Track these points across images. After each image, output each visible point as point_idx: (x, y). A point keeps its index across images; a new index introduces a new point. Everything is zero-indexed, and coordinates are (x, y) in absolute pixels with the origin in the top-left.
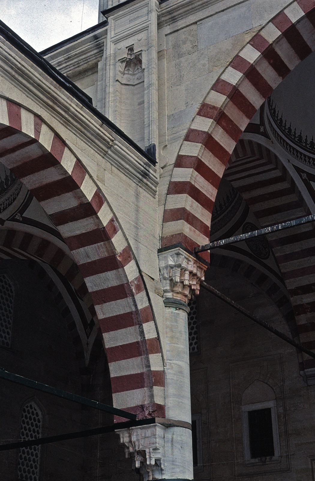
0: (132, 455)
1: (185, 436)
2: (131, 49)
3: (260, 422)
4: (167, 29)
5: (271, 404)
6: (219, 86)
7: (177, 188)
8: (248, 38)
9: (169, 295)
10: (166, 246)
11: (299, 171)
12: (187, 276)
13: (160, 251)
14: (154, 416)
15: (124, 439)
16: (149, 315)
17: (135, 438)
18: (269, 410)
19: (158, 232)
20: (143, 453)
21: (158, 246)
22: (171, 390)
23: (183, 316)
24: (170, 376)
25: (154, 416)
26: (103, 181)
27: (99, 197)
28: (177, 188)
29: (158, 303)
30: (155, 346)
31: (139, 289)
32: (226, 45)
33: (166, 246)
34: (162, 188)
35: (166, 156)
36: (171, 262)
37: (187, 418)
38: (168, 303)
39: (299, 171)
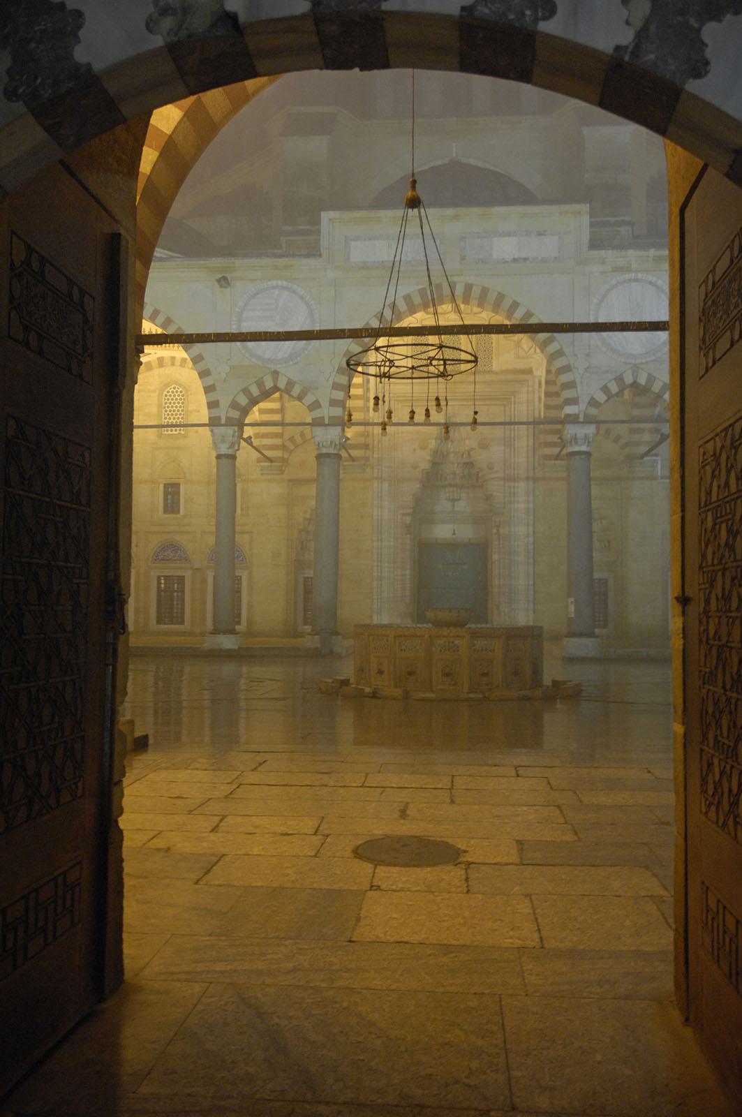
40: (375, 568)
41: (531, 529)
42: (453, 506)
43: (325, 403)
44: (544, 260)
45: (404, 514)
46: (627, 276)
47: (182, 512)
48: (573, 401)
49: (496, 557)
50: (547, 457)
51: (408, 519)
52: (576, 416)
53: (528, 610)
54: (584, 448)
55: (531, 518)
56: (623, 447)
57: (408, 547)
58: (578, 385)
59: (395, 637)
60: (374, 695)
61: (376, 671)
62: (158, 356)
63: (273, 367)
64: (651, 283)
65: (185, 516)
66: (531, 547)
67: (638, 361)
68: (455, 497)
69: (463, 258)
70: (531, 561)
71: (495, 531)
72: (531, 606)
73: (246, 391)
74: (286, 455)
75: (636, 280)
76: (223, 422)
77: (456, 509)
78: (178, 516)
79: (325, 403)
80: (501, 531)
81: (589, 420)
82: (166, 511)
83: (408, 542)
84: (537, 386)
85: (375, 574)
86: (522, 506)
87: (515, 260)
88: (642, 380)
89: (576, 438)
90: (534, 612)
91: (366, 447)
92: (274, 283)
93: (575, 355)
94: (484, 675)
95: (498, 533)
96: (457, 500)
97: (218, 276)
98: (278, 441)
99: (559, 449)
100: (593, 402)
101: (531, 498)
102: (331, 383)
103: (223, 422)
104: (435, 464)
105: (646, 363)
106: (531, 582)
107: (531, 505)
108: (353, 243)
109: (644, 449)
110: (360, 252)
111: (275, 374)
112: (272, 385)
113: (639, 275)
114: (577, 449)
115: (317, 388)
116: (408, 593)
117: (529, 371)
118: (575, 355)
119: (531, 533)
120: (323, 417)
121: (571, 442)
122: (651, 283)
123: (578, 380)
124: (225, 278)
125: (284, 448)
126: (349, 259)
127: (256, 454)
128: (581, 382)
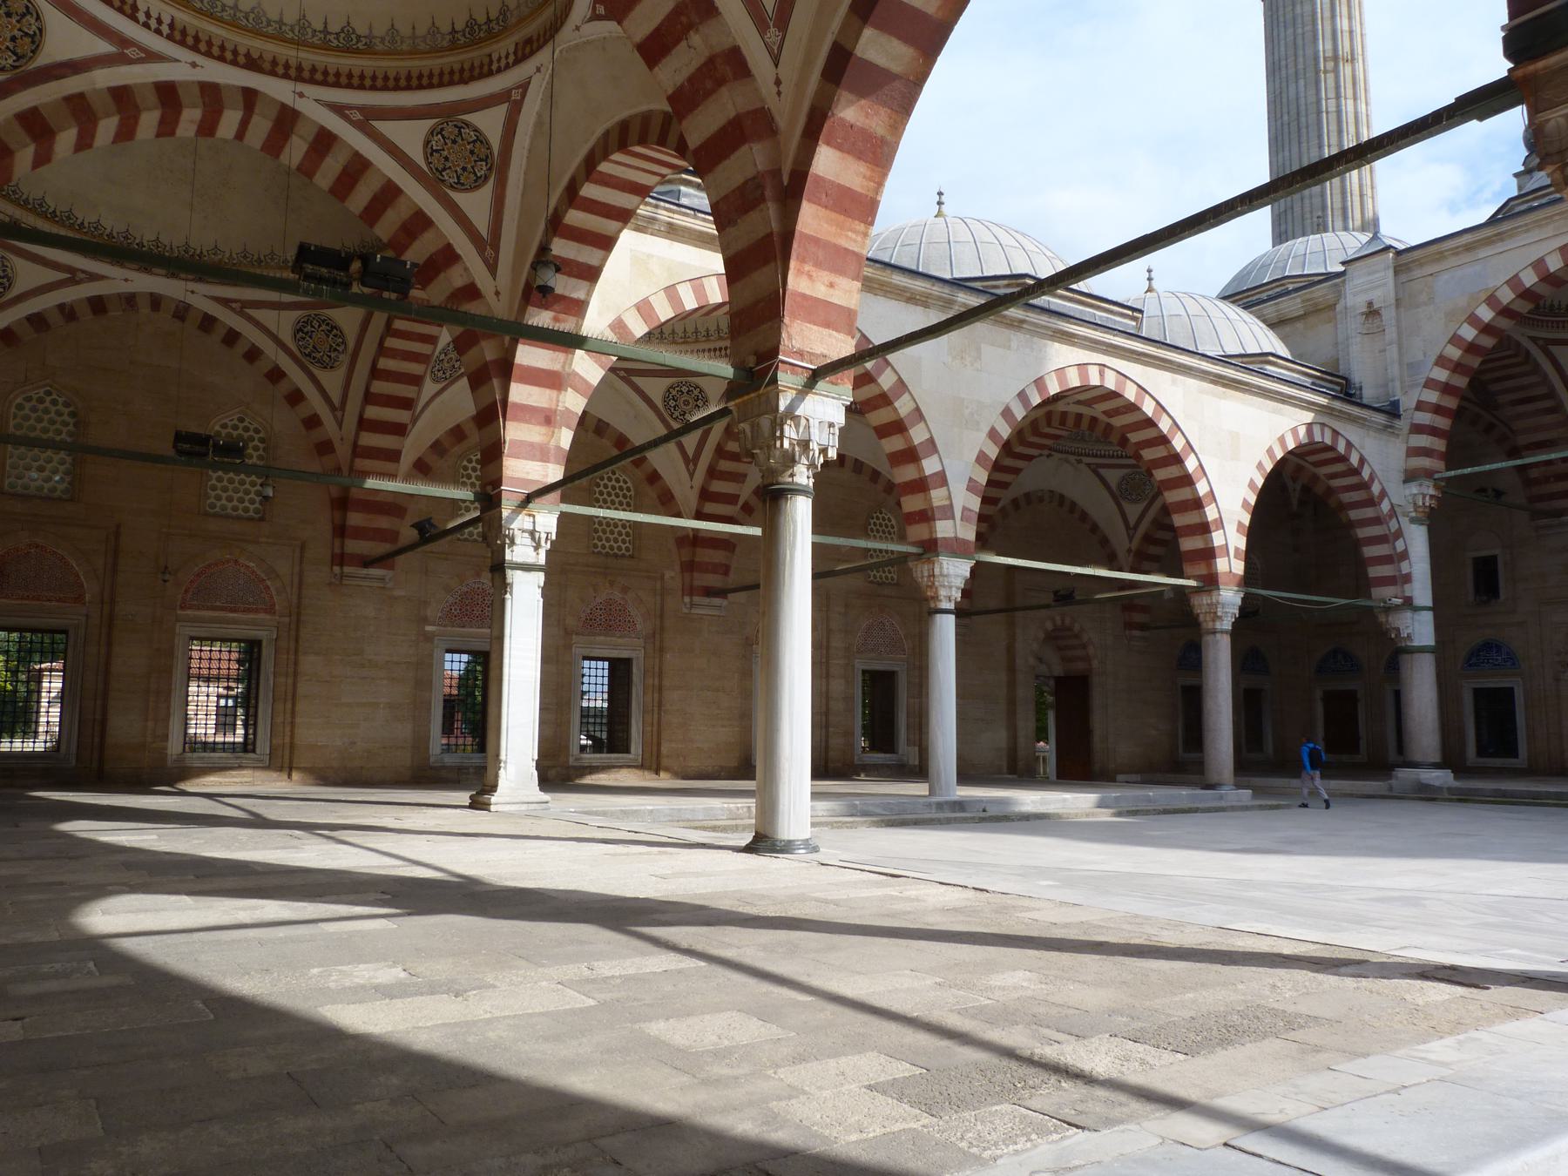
1: (1427, 618)
7: (1417, 429)
10: (1410, 477)
11: (1534, 339)
15: (1382, 618)
16: (1399, 534)
18: (1495, 557)
27: (1362, 461)
28: (1417, 429)
29: (1404, 521)
30: (1404, 556)
31: (1391, 517)
33: (1410, 477)
34: (1406, 429)
36: (1415, 491)
37: (1430, 604)
38: (1413, 521)
39: (1534, 339)
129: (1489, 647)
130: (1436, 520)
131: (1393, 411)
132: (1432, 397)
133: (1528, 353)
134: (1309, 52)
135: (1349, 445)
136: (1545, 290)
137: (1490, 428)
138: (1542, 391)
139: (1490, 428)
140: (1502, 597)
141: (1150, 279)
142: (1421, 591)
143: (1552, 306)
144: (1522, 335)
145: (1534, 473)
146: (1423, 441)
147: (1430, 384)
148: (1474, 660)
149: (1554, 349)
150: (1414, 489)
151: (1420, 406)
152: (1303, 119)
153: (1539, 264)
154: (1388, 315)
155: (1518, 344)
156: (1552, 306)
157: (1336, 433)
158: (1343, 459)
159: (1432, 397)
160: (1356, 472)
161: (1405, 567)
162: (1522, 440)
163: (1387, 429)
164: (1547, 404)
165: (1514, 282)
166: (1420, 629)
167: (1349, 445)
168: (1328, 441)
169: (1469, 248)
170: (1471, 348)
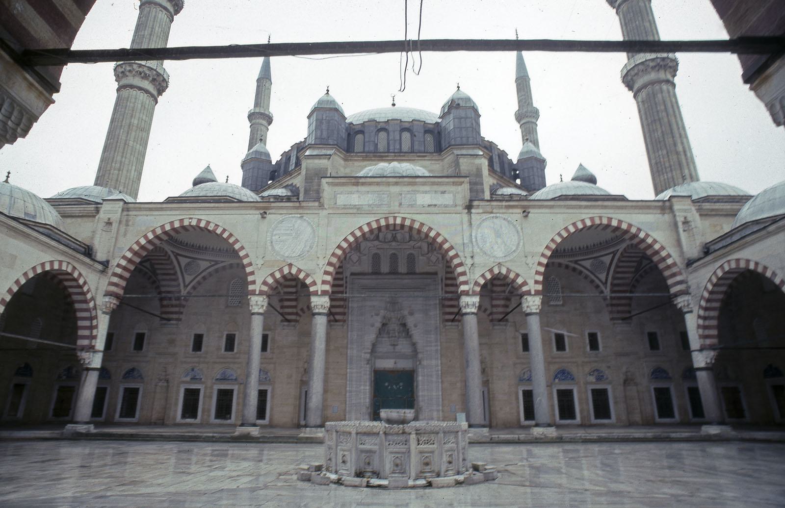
0: (81, 359)
1: (100, 355)
2: (109, 219)
3: (140, 338)
4: (125, 213)
5: (146, 331)
6: (138, 243)
7: (115, 275)
8: (152, 229)
9: (104, 310)
10: (108, 294)
11: (173, 252)
12: (112, 305)
13: (104, 296)
14: (91, 348)
15: (79, 354)
16: (96, 317)
17: (85, 355)
19: (105, 288)
20: (84, 359)
21: (104, 293)
22: (98, 340)
23: (107, 317)
24: (99, 336)
25: (91, 348)
26: (87, 277)
27: (85, 283)
28: (115, 275)
29: (99, 313)
30: (96, 327)
31: (93, 310)
32: (143, 229)
35: (113, 263)
38: (104, 313)
39: (173, 252)
40: (348, 386)
41: (439, 362)
42: (394, 349)
43: (319, 282)
44: (446, 206)
45: (365, 353)
46: (492, 215)
47: (235, 351)
48: (466, 283)
49: (420, 378)
50: (447, 321)
51: (368, 356)
52: (468, 291)
53: (438, 411)
54: (474, 310)
55: (439, 355)
56: (489, 315)
57: (368, 372)
58: (468, 274)
59: (357, 434)
60: (339, 482)
61: (341, 461)
62: (229, 263)
63: (289, 262)
64: (504, 219)
65: (236, 353)
66: (440, 372)
67: (501, 261)
68: (395, 343)
69: (400, 204)
70: (440, 380)
71: (418, 363)
72: (441, 408)
73: (272, 275)
74: (298, 318)
75: (497, 217)
76: (257, 293)
77: (397, 350)
78: (233, 353)
79: (319, 282)
80: (422, 363)
81: (474, 294)
82: (226, 350)
83: (368, 369)
84: (440, 282)
85: (348, 389)
86: (434, 348)
87: (429, 206)
88: (504, 271)
89: (468, 305)
90: (443, 411)
91: (344, 314)
92: (293, 215)
93: (465, 257)
94: (427, 464)
95: (420, 363)
96: (397, 345)
97: (262, 212)
98: (294, 310)
99: (454, 316)
100: (476, 284)
101: (439, 344)
102: (322, 271)
103: (257, 292)
104: (384, 325)
105: (506, 262)
106: (440, 394)
107: (439, 348)
108: (338, 195)
109: (501, 316)
110: (342, 200)
111: (290, 265)
112: (288, 272)
113: (498, 215)
114: (468, 310)
115: (314, 274)
116: (368, 400)
117: (436, 274)
118: (465, 257)
119: (439, 364)
120: (317, 291)
121: (465, 307)
122: (504, 219)
123: (468, 271)
124: (265, 213)
125: (297, 314)
126: (336, 203)
127: (280, 318)
128: (470, 272)
129: (133, 370)
130: (115, 315)
131: (106, 264)
132: (124, 263)
133: (169, 256)
134: (128, 121)
135: (80, 275)
136: (172, 233)
137: (154, 282)
138: (172, 272)
139: (154, 282)
140: (143, 350)
141: (8, 177)
142: (100, 344)
143: (181, 242)
144: (168, 248)
145: (165, 303)
146: (115, 280)
147: (124, 257)
148: (127, 375)
149: (179, 257)
150: (107, 299)
151: (119, 266)
152: (118, 144)
153: (172, 223)
154: (115, 226)
155: (166, 252)
156: (181, 242)
157: (74, 268)
158: (76, 280)
159: (124, 263)
160: (81, 287)
161: (95, 332)
162: (163, 289)
163: (103, 272)
164: (173, 277)
165: (162, 227)
166: (96, 361)
167: (80, 275)
168: (69, 270)
169: (151, 209)
170: (142, 247)
